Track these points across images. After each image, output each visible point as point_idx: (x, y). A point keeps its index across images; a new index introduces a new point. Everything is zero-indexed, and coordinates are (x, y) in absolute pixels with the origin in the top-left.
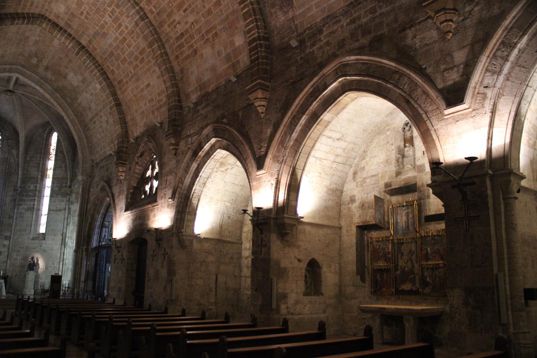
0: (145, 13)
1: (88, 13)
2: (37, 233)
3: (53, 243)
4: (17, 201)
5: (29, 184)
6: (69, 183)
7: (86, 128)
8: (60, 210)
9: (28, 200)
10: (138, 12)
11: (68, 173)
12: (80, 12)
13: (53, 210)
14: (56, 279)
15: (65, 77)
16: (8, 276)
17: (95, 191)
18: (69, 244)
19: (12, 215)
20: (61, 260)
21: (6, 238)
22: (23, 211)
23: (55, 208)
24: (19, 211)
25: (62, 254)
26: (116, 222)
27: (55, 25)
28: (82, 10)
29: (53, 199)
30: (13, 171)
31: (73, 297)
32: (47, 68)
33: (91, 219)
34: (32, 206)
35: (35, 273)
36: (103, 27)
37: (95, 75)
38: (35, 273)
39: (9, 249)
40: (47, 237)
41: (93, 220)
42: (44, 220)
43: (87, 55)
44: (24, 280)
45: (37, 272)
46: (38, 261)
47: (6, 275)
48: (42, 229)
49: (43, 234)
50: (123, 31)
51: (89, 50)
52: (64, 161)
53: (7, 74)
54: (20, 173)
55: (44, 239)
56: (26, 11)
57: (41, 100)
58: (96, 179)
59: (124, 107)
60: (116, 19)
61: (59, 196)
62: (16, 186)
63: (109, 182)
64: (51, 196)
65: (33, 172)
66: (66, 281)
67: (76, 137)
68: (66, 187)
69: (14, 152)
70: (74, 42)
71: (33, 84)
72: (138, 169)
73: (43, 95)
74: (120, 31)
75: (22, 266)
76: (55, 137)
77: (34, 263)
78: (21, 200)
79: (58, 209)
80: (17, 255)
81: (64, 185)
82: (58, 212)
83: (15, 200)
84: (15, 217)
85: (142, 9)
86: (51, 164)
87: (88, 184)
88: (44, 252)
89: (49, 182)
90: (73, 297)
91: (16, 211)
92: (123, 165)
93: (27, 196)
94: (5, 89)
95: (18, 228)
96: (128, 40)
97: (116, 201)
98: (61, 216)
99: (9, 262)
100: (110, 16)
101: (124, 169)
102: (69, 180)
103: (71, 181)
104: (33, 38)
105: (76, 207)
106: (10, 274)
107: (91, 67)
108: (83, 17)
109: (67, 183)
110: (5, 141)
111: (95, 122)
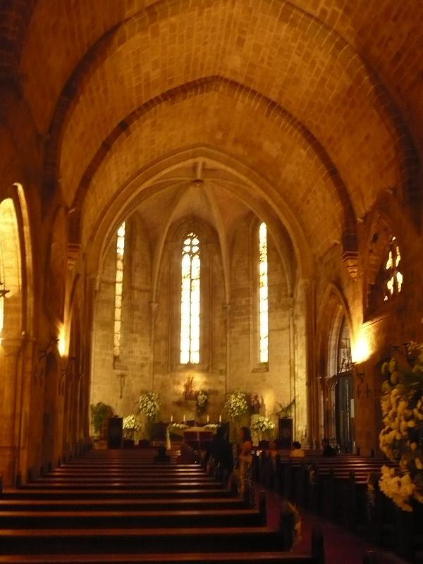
0: (341, 38)
1: (270, 58)
2: (258, 362)
3: (279, 374)
4: (228, 323)
5: (239, 299)
6: (289, 291)
7: (298, 211)
8: (283, 329)
9: (241, 320)
10: (331, 40)
11: (287, 276)
12: (259, 59)
13: (274, 330)
14: (285, 423)
15: (260, 148)
17: (324, 297)
18: (299, 375)
19: (224, 341)
21: (221, 372)
22: (237, 335)
23: (276, 328)
24: (233, 335)
25: (292, 389)
26: (354, 341)
27: (234, 84)
28: (261, 55)
31: (311, 447)
32: (236, 142)
33: (323, 337)
36: (292, 70)
37: (295, 137)
39: (226, 386)
41: (326, 339)
42: (264, 344)
43: (281, 113)
50: (319, 70)
51: (282, 105)
52: (278, 260)
53: (190, 162)
55: (268, 370)
56: (198, 77)
57: (237, 184)
58: (322, 281)
59: (342, 174)
60: (307, 55)
62: (224, 303)
63: (338, 284)
64: (270, 311)
65: (243, 282)
66: (301, 425)
67: (288, 227)
68: (286, 295)
69: (216, 258)
70: (261, 99)
71: (223, 167)
72: (373, 259)
73: (237, 178)
74: (315, 69)
76: (263, 230)
77: (258, 403)
81: (283, 294)
82: (281, 332)
83: (225, 321)
84: (228, 344)
85: (336, 33)
86: (263, 267)
87: (313, 288)
89: (263, 292)
90: (311, 447)
91: (228, 336)
92: (353, 256)
93: (240, 314)
94: (194, 179)
96: (329, 79)
97: (351, 309)
98: (285, 336)
100: (299, 55)
101: (355, 262)
102: (289, 286)
104: (212, 108)
105: (301, 323)
107: (288, 128)
108: (265, 65)
109: (286, 291)
111: (308, 202)
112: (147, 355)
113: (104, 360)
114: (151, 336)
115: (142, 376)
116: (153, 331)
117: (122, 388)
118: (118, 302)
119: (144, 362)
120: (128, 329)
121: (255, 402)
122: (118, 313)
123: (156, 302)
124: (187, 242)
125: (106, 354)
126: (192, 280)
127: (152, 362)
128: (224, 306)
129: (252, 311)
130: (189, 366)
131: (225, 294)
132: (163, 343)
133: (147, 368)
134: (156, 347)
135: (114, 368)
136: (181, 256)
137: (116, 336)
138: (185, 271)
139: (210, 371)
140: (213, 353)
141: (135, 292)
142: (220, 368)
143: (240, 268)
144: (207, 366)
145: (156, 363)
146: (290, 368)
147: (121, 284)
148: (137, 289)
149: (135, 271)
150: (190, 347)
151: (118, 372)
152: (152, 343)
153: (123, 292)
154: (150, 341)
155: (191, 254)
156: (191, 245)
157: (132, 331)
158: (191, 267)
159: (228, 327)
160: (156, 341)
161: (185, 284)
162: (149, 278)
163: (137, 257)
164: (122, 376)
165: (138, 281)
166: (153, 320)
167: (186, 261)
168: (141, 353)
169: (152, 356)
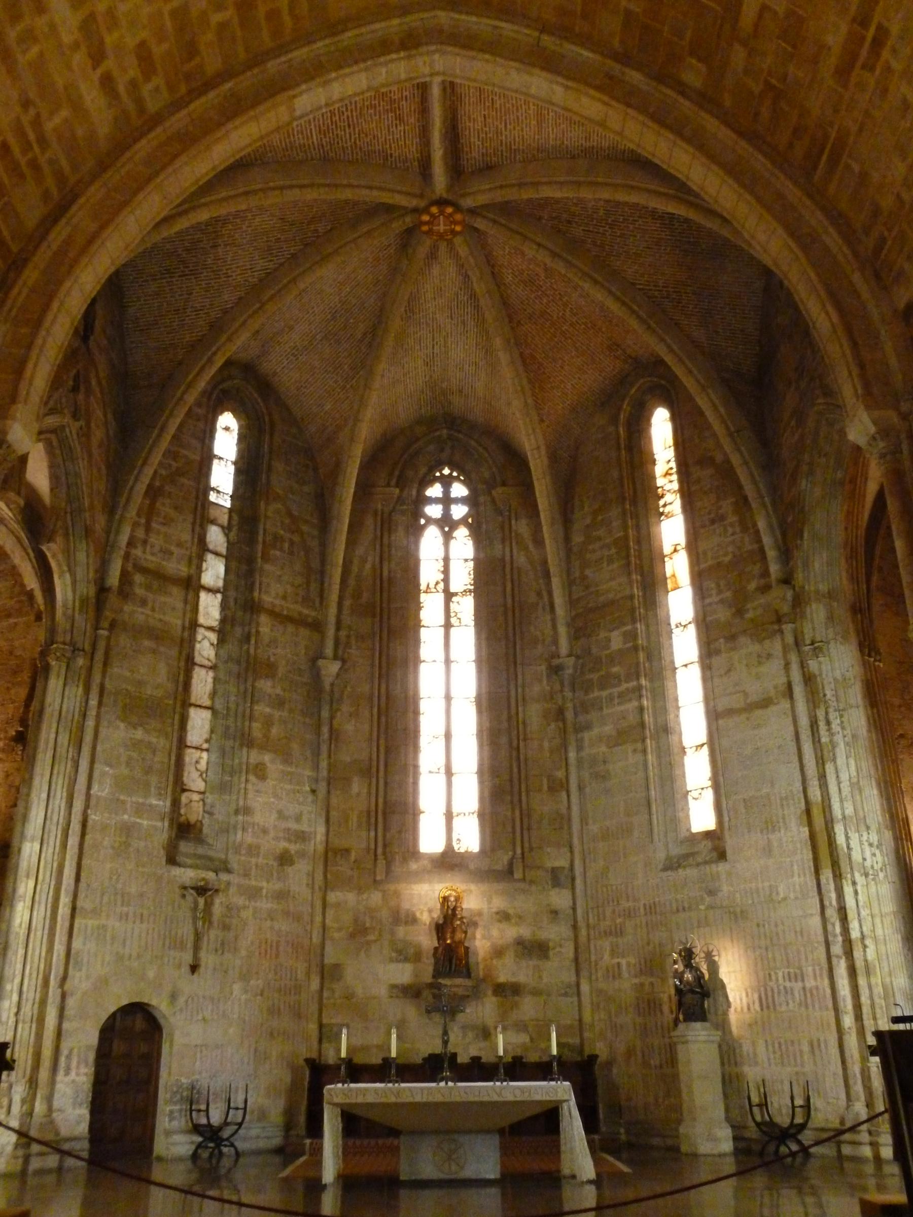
2: (683, 834)
3: (776, 866)
4: (569, 715)
5: (603, 634)
6: (774, 568)
8: (765, 703)
9: (611, 698)
13: (730, 712)
16: (593, 1058)
18: (856, 856)
19: (560, 774)
23: (737, 701)
25: (832, 913)
29: (716, 661)
30: (533, 598)
34: (632, 719)
35: (716, 1036)
38: (716, 1036)
39: (575, 927)
40: (730, 843)
42: (697, 770)
45: (723, 1025)
46: (714, 968)
47: (587, 1051)
48: (702, 816)
49: (708, 834)
54: (559, 600)
55: (722, 856)
61: (743, 640)
65: (610, 582)
75: (648, 1005)
77: (699, 978)
78: (583, 708)
79: (753, 698)
80: (613, 953)
81: (752, 586)
83: (560, 713)
86: (672, 531)
88: (736, 918)
89: (680, 604)
91: (572, 755)
95: (594, 828)
98: (776, 726)
99: (585, 987)
102: (771, 554)
103: (786, 554)
106: (601, 1049)
110: (482, 499)
112: (304, 827)
113: (127, 830)
114: (316, 767)
115: (281, 896)
116: (324, 748)
117: (198, 937)
119: (293, 848)
120: (234, 734)
122: (202, 683)
123: (335, 657)
124: (435, 491)
125: (139, 810)
126: (449, 596)
127: (321, 848)
128: (555, 662)
129: (651, 663)
130: (449, 861)
131: (554, 627)
132: (357, 786)
134: (334, 801)
135: (172, 860)
136: (416, 531)
137: (190, 756)
138: (429, 572)
139: (518, 875)
140: (526, 814)
141: (264, 619)
142: (549, 864)
143: (597, 545)
144: (506, 859)
145: (332, 854)
146: (812, 836)
147: (219, 596)
148: (274, 614)
149: (266, 558)
150: (448, 794)
151: (187, 875)
152: (322, 788)
153: (223, 621)
155: (447, 525)
157: (248, 742)
158: (445, 558)
159: (570, 729)
160: (336, 779)
161: (431, 608)
162: (314, 586)
163: (272, 518)
164: (201, 890)
165: (276, 587)
166: (325, 714)
167: (430, 544)
168: (281, 815)
169: (321, 829)
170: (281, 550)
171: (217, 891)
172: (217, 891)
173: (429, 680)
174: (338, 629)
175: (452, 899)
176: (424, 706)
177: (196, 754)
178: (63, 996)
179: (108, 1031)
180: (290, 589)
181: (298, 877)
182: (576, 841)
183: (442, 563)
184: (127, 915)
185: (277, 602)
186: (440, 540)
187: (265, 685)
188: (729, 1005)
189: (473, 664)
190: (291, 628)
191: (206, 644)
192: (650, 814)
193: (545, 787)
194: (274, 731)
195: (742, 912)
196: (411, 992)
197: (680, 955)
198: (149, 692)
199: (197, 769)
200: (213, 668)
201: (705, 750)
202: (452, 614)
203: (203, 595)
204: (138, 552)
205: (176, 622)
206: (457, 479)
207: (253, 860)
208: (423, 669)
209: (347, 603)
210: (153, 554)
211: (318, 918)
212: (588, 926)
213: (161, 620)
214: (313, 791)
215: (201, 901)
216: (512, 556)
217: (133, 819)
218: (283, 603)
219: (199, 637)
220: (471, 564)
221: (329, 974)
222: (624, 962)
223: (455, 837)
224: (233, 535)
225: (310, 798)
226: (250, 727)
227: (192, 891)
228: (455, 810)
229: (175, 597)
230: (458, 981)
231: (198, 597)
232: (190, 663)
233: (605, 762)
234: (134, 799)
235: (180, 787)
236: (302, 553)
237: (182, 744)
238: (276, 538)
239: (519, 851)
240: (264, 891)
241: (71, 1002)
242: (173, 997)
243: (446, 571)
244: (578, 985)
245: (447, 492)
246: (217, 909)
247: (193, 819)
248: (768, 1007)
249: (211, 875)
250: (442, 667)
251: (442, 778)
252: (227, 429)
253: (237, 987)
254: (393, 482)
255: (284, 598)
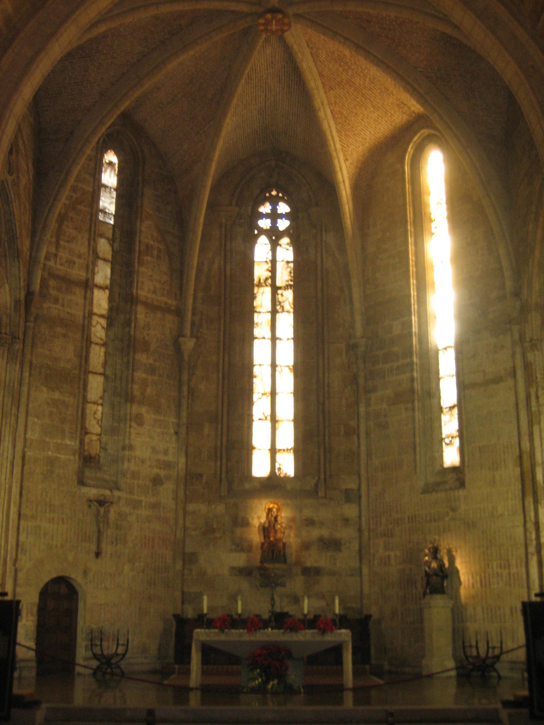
4: (361, 381)
8: (497, 380)
13: (473, 385)
16: (368, 617)
19: (353, 423)
20: (532, 549)
21: (350, 496)
35: (450, 603)
39: (360, 530)
42: (450, 425)
44: (417, 628)
45: (456, 596)
46: (452, 560)
47: (365, 612)
48: (451, 456)
49: (454, 469)
55: (462, 484)
77: (441, 566)
80: (386, 548)
83: (354, 379)
91: (362, 409)
99: (365, 571)
106: (374, 611)
112: (170, 458)
113: (51, 462)
114: (179, 416)
115: (155, 506)
116: (184, 402)
117: (99, 533)
118: (99, 330)
119: (162, 473)
120: (121, 393)
121: (434, 565)
122: (97, 356)
123: (192, 336)
124: (266, 209)
126: (275, 289)
127: (182, 473)
130: (273, 484)
133: (169, 486)
135: (81, 482)
136: (252, 240)
137: (90, 408)
138: (260, 271)
142: (344, 487)
144: (313, 482)
145: (191, 477)
146: (522, 473)
147: (107, 292)
148: (146, 304)
149: (140, 263)
151: (92, 492)
152: (183, 430)
154: (178, 425)
156: (274, 216)
157: (130, 399)
161: (263, 299)
164: (101, 502)
166: (185, 377)
167: (262, 249)
168: (154, 450)
169: (183, 460)
170: (152, 256)
171: (112, 503)
172: (112, 503)
173: (260, 351)
174: (193, 314)
175: (275, 510)
176: (256, 370)
177: (94, 407)
178: (16, 571)
179: (44, 594)
180: (158, 285)
181: (166, 494)
182: (363, 472)
183: (270, 265)
184: (53, 519)
185: (149, 295)
186: (269, 247)
187: (142, 358)
188: (460, 583)
189: (292, 395)
190: (159, 315)
191: (99, 327)
192: (415, 454)
193: (342, 433)
194: (148, 391)
195: (473, 523)
196: (245, 572)
197: (429, 550)
198: (62, 365)
199: (95, 418)
200: (105, 345)
201: (456, 411)
202: (277, 303)
203: (96, 292)
204: (51, 263)
205: (79, 313)
206: (282, 199)
207: (136, 482)
208: (256, 344)
209: (200, 294)
210: (62, 264)
211: (181, 522)
212: (369, 531)
213: (68, 313)
214: (176, 433)
215: (102, 510)
216: (322, 261)
217: (55, 454)
218: (154, 296)
219: (94, 323)
220: (292, 265)
221: (190, 559)
222: (392, 554)
223: (277, 466)
224: (116, 245)
225: (174, 438)
226: (132, 388)
227: (95, 503)
228: (278, 446)
229: (78, 296)
230: (277, 566)
231: (93, 293)
232: (88, 342)
233: (385, 416)
234: (55, 441)
235: (85, 431)
236: (167, 257)
237: (85, 401)
238: (148, 246)
239: (322, 477)
240: (143, 504)
241: (21, 575)
242: (85, 573)
243: (273, 271)
244: (360, 569)
245: (274, 210)
246: (112, 516)
247: (93, 453)
248: (485, 585)
249: (108, 492)
250: (269, 343)
251: (268, 424)
252: (111, 164)
253: (127, 568)
254: (234, 203)
255: (154, 292)
